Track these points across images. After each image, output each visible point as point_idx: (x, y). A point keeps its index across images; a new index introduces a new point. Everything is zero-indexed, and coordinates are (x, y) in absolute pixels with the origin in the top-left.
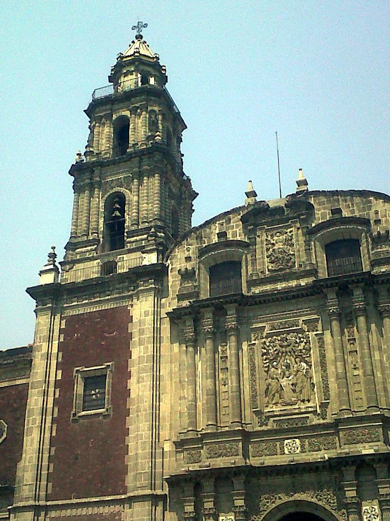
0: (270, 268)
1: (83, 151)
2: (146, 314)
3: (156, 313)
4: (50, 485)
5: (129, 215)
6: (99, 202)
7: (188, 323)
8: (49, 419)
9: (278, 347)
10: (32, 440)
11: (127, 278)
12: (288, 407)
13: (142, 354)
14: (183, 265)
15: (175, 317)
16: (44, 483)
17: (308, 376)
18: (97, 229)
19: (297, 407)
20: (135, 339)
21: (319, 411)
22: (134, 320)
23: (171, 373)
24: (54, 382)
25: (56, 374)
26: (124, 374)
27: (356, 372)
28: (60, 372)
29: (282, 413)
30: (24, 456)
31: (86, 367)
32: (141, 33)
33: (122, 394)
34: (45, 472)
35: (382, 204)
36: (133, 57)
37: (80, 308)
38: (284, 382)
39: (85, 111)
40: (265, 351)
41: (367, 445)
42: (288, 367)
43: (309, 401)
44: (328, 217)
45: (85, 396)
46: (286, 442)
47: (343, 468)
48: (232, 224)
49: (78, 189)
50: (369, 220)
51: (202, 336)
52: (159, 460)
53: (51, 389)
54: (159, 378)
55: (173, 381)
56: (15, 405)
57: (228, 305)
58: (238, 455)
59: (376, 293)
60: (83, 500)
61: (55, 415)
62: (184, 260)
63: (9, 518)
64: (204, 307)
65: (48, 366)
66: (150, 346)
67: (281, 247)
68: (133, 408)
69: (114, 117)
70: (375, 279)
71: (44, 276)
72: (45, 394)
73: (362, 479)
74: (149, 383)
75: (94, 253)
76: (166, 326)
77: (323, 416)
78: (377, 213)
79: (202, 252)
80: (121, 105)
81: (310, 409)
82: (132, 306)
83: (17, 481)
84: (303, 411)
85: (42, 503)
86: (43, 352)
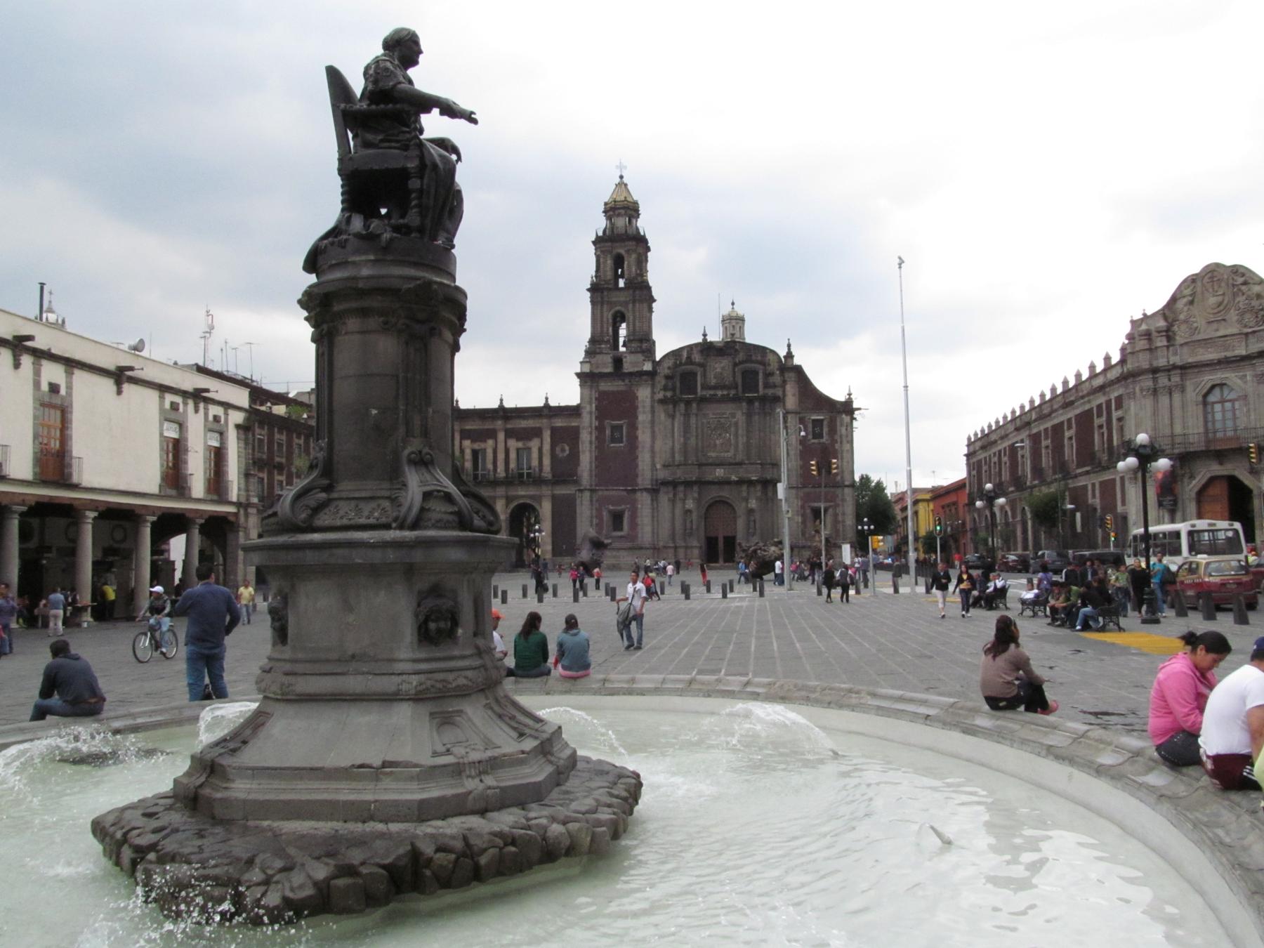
1: (594, 274)
3: (652, 397)
8: (594, 446)
15: (663, 401)
18: (608, 333)
20: (640, 409)
26: (633, 427)
30: (581, 464)
33: (633, 439)
34: (594, 473)
37: (605, 386)
38: (718, 442)
42: (720, 435)
49: (593, 302)
53: (594, 431)
63: (575, 494)
66: (650, 416)
72: (591, 433)
77: (735, 459)
85: (593, 487)
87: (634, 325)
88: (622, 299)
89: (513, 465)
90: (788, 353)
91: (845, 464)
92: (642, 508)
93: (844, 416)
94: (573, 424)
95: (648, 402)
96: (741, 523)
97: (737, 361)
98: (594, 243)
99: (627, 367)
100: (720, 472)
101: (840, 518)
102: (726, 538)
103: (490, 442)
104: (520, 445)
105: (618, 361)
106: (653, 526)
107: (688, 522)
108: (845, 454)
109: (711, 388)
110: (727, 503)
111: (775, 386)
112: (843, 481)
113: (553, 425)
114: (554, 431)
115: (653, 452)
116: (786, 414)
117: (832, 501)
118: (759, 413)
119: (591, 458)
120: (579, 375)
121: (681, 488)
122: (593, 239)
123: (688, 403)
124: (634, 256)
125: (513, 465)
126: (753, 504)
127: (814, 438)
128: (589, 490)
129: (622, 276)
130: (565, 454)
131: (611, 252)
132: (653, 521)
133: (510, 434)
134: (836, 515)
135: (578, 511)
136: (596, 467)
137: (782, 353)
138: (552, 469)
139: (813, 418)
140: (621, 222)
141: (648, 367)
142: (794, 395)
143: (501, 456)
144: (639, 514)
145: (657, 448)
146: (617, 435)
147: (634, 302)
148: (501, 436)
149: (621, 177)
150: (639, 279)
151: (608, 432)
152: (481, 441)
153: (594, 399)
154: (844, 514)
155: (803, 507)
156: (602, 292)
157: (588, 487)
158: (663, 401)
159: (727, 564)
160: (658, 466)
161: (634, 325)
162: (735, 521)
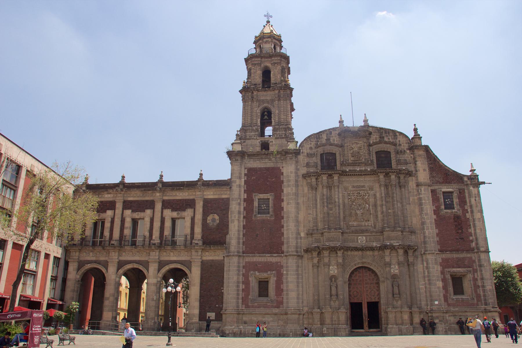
0: (352, 159)
1: (246, 81)
2: (291, 172)
3: (296, 173)
4: (244, 247)
5: (273, 119)
8: (242, 216)
9: (356, 196)
10: (234, 226)
11: (280, 153)
13: (290, 192)
14: (308, 151)
15: (304, 176)
17: (369, 210)
18: (256, 124)
19: (363, 223)
21: (373, 226)
22: (284, 174)
23: (304, 202)
24: (243, 199)
25: (244, 196)
26: (279, 200)
27: (390, 211)
28: (246, 195)
30: (230, 233)
31: (261, 194)
32: (269, 20)
33: (279, 209)
34: (241, 241)
35: (402, 138)
36: (270, 34)
38: (358, 212)
39: (245, 59)
40: (350, 197)
41: (395, 241)
43: (369, 221)
44: (378, 139)
45: (259, 207)
46: (359, 237)
47: (385, 250)
48: (332, 135)
49: (244, 100)
50: (396, 145)
51: (320, 186)
53: (242, 202)
54: (298, 204)
55: (305, 206)
57: (335, 175)
58: (339, 241)
60: (262, 255)
61: (245, 215)
62: (308, 149)
63: (224, 260)
65: (240, 191)
66: (294, 188)
67: (357, 150)
68: (285, 216)
69: (262, 65)
70: (400, 172)
71: (235, 145)
73: (392, 255)
74: (294, 205)
75: (256, 137)
76: (301, 179)
77: (375, 227)
78: (399, 141)
79: (317, 147)
80: (267, 60)
81: (370, 225)
82: (283, 167)
83: (227, 243)
84: (366, 225)
85: (241, 254)
86: (237, 184)
87: (279, 118)
88: (269, 98)
89: (167, 232)
91: (478, 231)
92: (287, 274)
93: (471, 188)
94: (224, 196)
95: (292, 177)
96: (384, 287)
97: (371, 143)
99: (273, 148)
100: (362, 240)
101: (479, 283)
103: (149, 212)
104: (175, 214)
106: (298, 290)
107: (333, 289)
108: (477, 222)
109: (349, 165)
110: (369, 269)
111: (406, 163)
112: (478, 248)
113: (206, 197)
114: (207, 203)
115: (297, 221)
116: (418, 185)
117: (469, 267)
120: (230, 154)
121: (326, 253)
122: (246, 57)
124: (279, 67)
126: (395, 269)
127: (445, 209)
128: (236, 256)
130: (215, 224)
131: (260, 64)
132: (298, 286)
133: (166, 205)
134: (475, 280)
135: (225, 276)
136: (244, 235)
137: (411, 135)
138: (203, 237)
139: (443, 190)
140: (268, 47)
142: (424, 170)
143: (157, 225)
144: (284, 281)
145: (301, 217)
146: (264, 207)
147: (279, 100)
148: (158, 206)
149: (268, 22)
150: (283, 83)
151: (256, 204)
152: (141, 211)
153: (243, 175)
154: (482, 279)
155: (442, 273)
156: (253, 93)
157: (236, 254)
159: (371, 330)
160: (302, 235)
161: (279, 118)
162: (379, 287)
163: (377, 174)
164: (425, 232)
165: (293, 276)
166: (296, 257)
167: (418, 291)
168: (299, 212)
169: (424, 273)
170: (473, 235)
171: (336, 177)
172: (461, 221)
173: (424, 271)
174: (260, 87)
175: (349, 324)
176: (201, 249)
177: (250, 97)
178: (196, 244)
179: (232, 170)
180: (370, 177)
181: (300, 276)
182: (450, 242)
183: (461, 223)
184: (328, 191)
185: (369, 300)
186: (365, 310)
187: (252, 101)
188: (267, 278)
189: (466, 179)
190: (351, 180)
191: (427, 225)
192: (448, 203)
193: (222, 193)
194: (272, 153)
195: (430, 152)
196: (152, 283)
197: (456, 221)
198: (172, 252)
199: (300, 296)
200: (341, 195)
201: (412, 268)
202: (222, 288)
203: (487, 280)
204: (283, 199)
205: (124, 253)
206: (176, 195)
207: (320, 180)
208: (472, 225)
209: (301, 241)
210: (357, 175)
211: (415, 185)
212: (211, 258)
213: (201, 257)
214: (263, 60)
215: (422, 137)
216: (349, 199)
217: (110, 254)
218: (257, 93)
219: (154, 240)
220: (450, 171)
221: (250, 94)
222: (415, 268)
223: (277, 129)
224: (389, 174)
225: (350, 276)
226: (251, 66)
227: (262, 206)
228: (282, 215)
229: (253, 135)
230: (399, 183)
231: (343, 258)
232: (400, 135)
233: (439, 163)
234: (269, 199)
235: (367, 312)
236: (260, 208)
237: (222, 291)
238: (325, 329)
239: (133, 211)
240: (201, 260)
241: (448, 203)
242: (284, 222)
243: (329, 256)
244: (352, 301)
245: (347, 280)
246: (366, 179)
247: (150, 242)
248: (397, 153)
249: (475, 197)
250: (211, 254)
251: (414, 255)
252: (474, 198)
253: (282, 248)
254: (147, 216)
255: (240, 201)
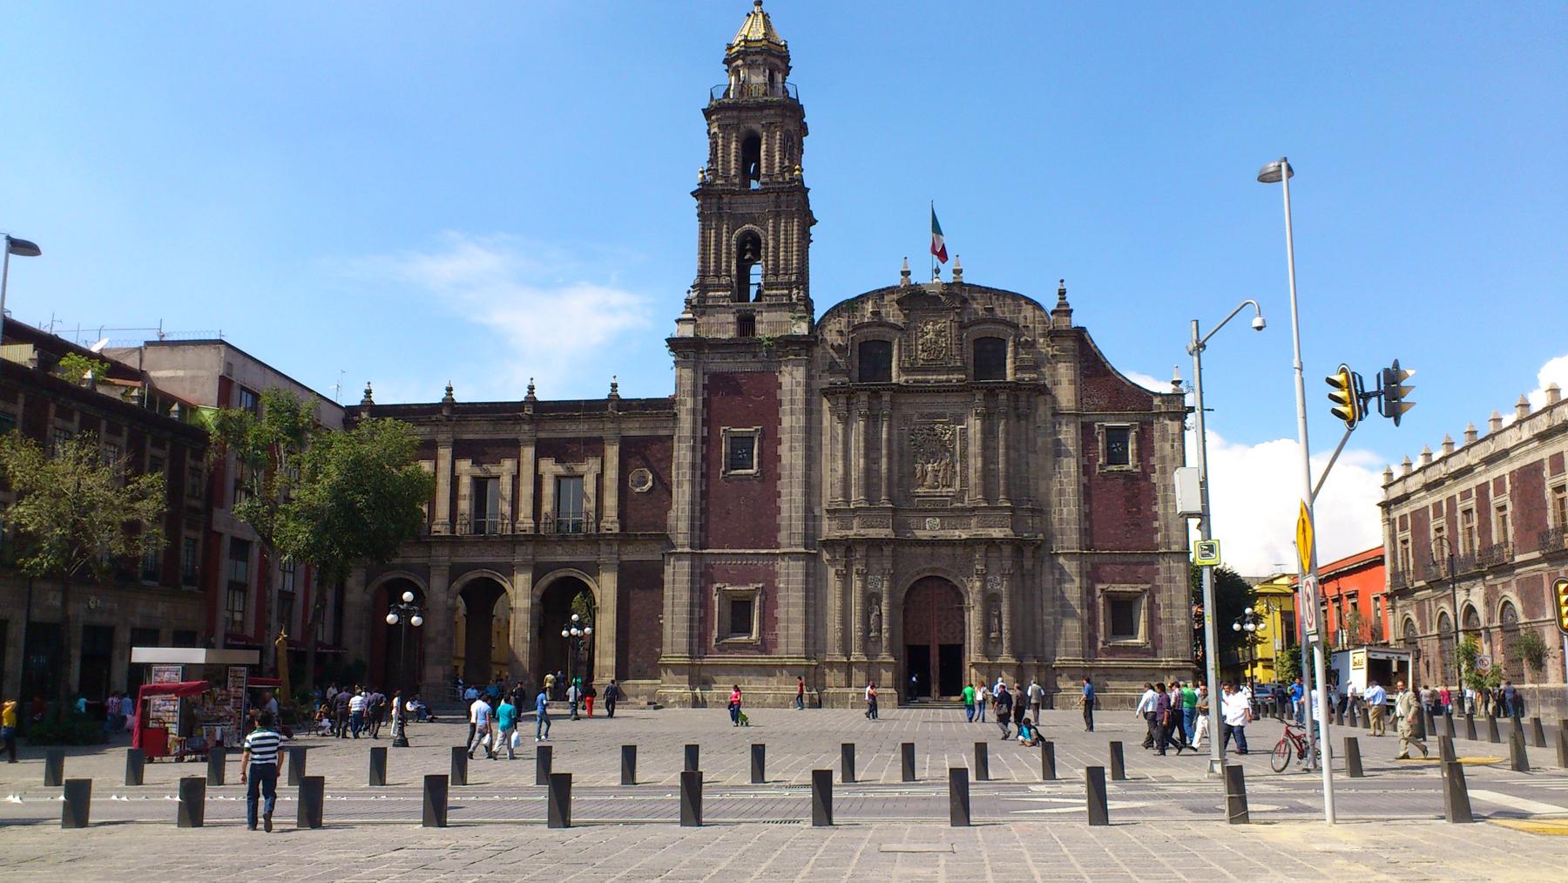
6: (730, 240)
7: (841, 401)
9: (926, 436)
10: (684, 492)
12: (931, 490)
14: (834, 338)
16: (697, 532)
19: (938, 490)
20: (786, 407)
26: (771, 438)
29: (926, 494)
33: (770, 460)
34: (697, 523)
39: (703, 110)
41: (997, 530)
45: (732, 453)
46: (928, 520)
52: (811, 523)
56: (659, 456)
59: (1017, 397)
64: (861, 390)
65: (695, 422)
66: (802, 418)
69: (742, 129)
73: (989, 555)
84: (944, 494)
86: (688, 407)
89: (547, 507)
90: (1059, 305)
98: (708, 113)
102: (941, 646)
103: (508, 465)
104: (560, 470)
105: (746, 323)
106: (807, 621)
112: (1168, 545)
117: (1147, 583)
118: (1006, 415)
119: (693, 495)
120: (674, 344)
122: (706, 107)
123: (875, 394)
125: (547, 507)
127: (1109, 463)
129: (757, 176)
133: (543, 450)
137: (1050, 303)
139: (1106, 424)
141: (802, 329)
143: (527, 490)
144: (781, 601)
157: (687, 550)
158: (829, 393)
163: (971, 391)
164: (1062, 510)
165: (798, 594)
166: (803, 556)
167: (1039, 626)
168: (812, 466)
169: (1054, 592)
170: (1161, 517)
171: (886, 398)
172: (1139, 489)
173: (1054, 588)
174: (735, 185)
175: (901, 686)
176: (617, 540)
177: (715, 210)
178: (607, 530)
179: (679, 378)
180: (957, 396)
181: (812, 594)
182: (1112, 532)
183: (1139, 494)
184: (871, 424)
185: (944, 642)
186: (935, 661)
187: (720, 217)
188: (748, 597)
189: (1156, 401)
190: (917, 401)
191: (1067, 497)
192: (1115, 450)
193: (658, 424)
194: (760, 342)
195: (1089, 341)
196: (522, 607)
197: (1126, 489)
198: (560, 546)
199: (811, 633)
200: (895, 432)
201: (1029, 583)
202: (660, 616)
203: (1178, 608)
204: (780, 438)
205: (461, 549)
206: (564, 430)
207: (855, 401)
208: (1160, 500)
209: (814, 525)
210: (929, 391)
211: (1049, 413)
212: (638, 557)
213: (619, 555)
214: (744, 114)
215: (1071, 311)
216: (913, 440)
217: (433, 552)
218: (730, 199)
219: (522, 523)
220: (1127, 383)
221: (714, 201)
222: (1037, 581)
223: (773, 284)
224: (994, 390)
225: (908, 594)
226: (716, 130)
227: (740, 452)
228: (778, 471)
229: (721, 297)
230: (1016, 409)
231: (894, 561)
232: (1026, 303)
233: (1105, 366)
234: (753, 437)
235: (937, 664)
236: (735, 456)
237: (661, 621)
238: (855, 695)
239: (476, 463)
240: (618, 562)
241: (1115, 450)
242: (783, 486)
243: (867, 556)
244: (911, 643)
245: (901, 602)
246: (948, 400)
247: (513, 525)
248: (1017, 345)
249: (1173, 440)
250: (638, 549)
251: (1037, 556)
252: (1170, 442)
253: (776, 538)
254: (504, 474)
255: (694, 442)
